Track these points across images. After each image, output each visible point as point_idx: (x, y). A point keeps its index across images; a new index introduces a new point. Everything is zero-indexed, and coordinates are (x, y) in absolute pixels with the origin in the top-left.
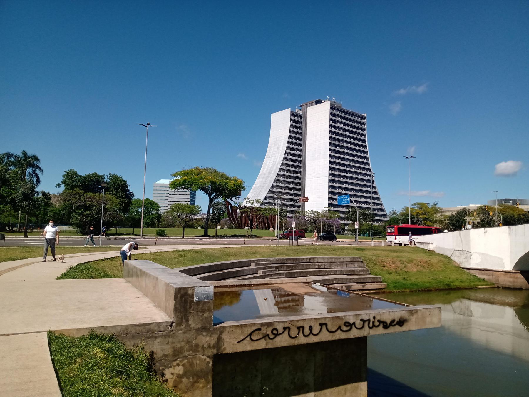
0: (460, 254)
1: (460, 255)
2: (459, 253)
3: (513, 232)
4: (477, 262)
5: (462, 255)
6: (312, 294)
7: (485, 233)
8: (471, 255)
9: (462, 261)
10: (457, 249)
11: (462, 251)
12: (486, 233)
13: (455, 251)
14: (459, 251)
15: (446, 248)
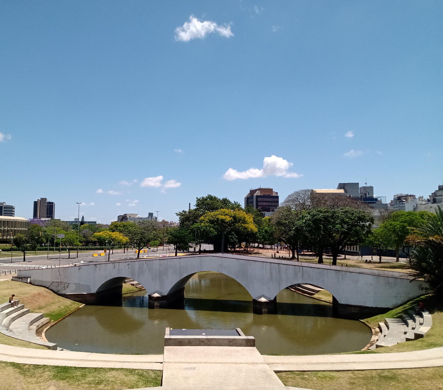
0: (58, 285)
1: (57, 286)
2: (57, 284)
3: (98, 269)
4: (73, 290)
5: (60, 285)
6: (70, 360)
7: (79, 269)
8: (68, 285)
9: (59, 289)
10: (56, 281)
11: (60, 282)
12: (80, 270)
13: (53, 283)
14: (57, 283)
15: (44, 280)
